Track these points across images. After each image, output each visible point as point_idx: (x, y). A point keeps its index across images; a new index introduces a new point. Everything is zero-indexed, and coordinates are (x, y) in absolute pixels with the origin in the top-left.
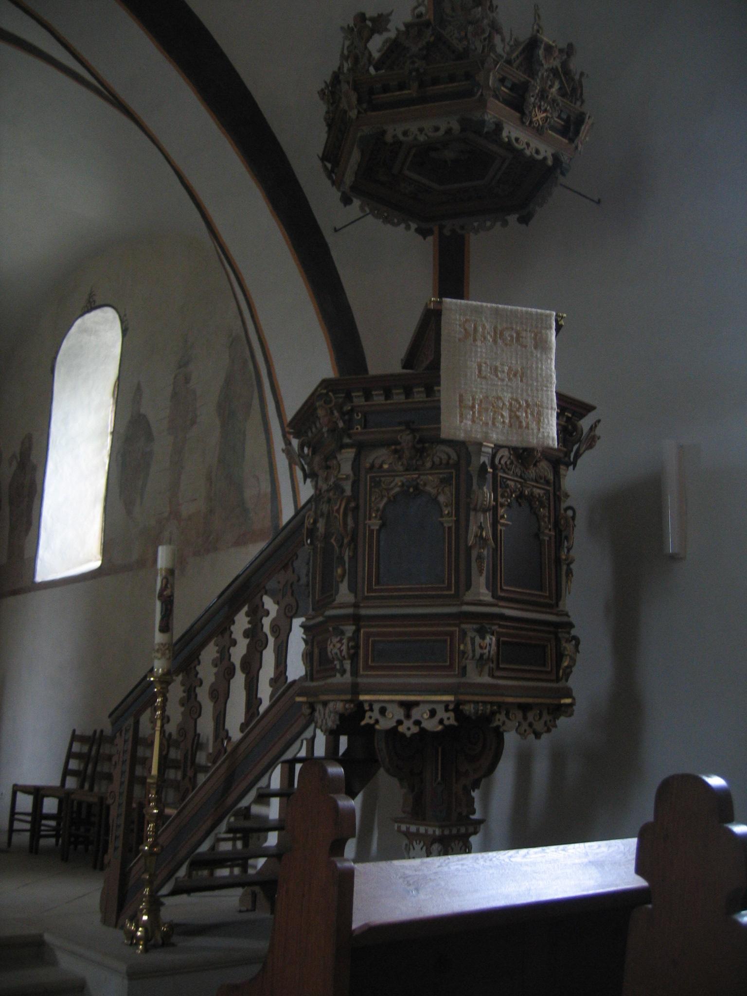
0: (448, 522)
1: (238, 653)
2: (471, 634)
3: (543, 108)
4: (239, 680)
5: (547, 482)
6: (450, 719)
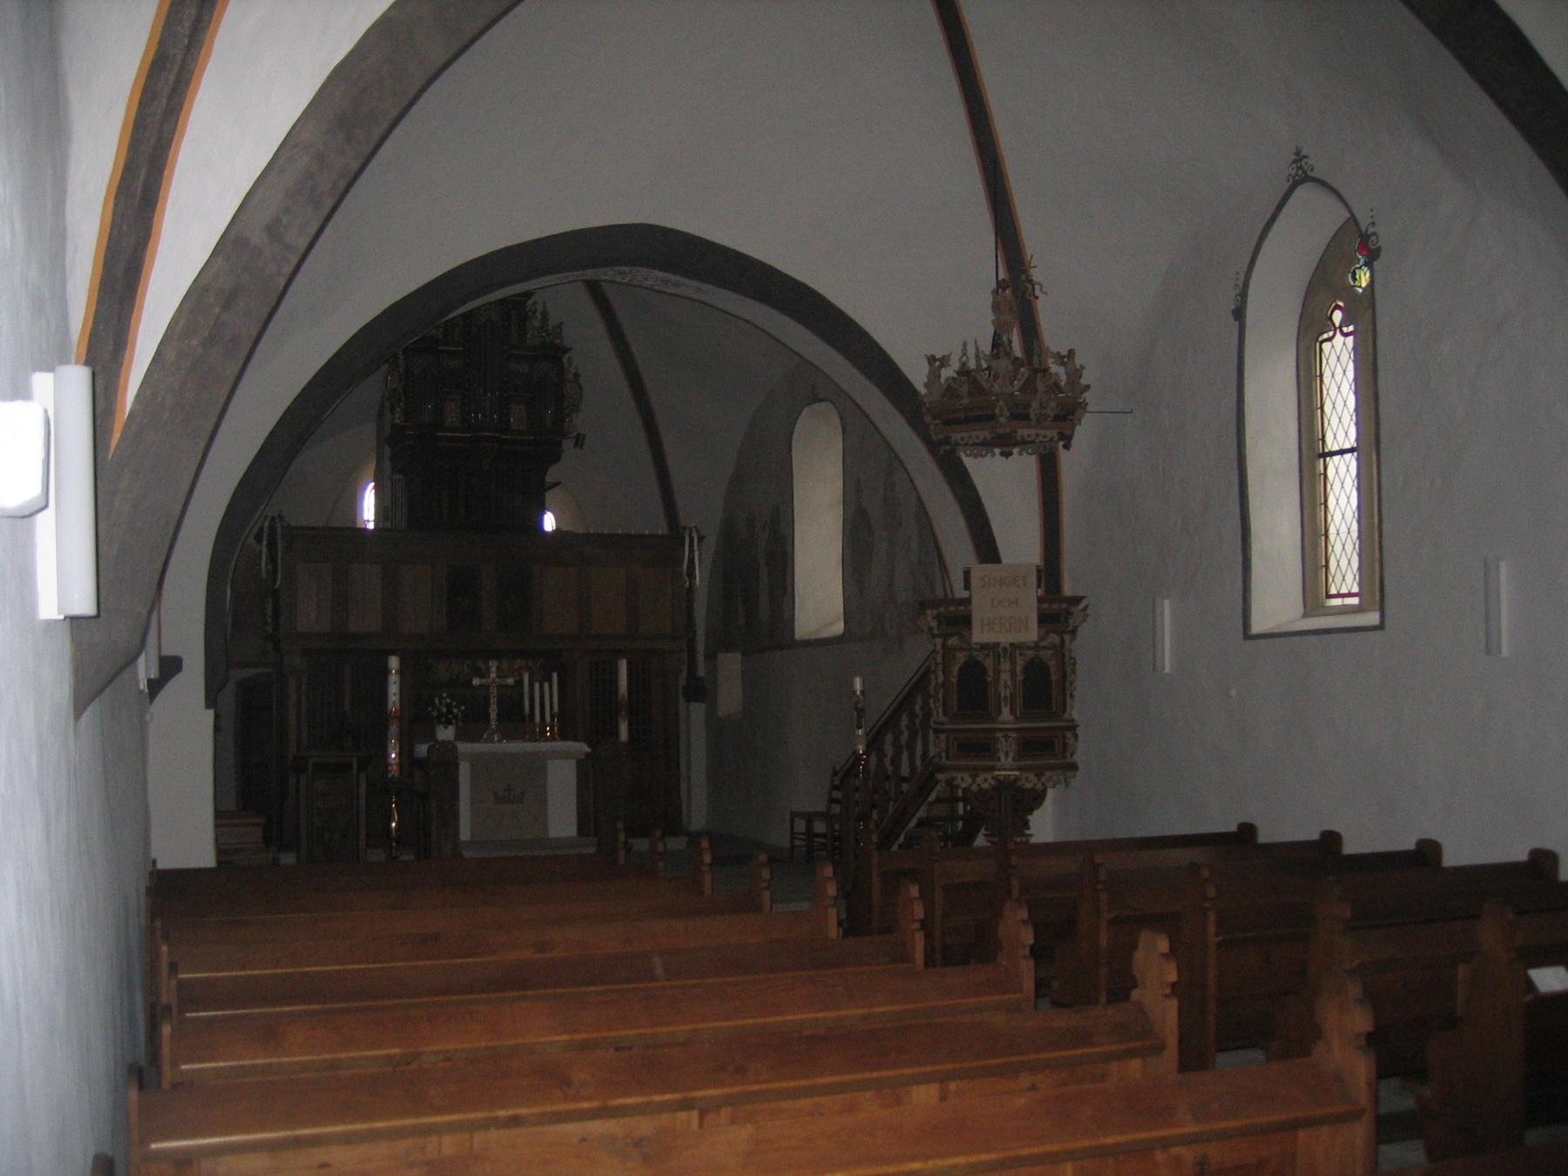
1: (904, 739)
4: (905, 756)
6: (993, 782)
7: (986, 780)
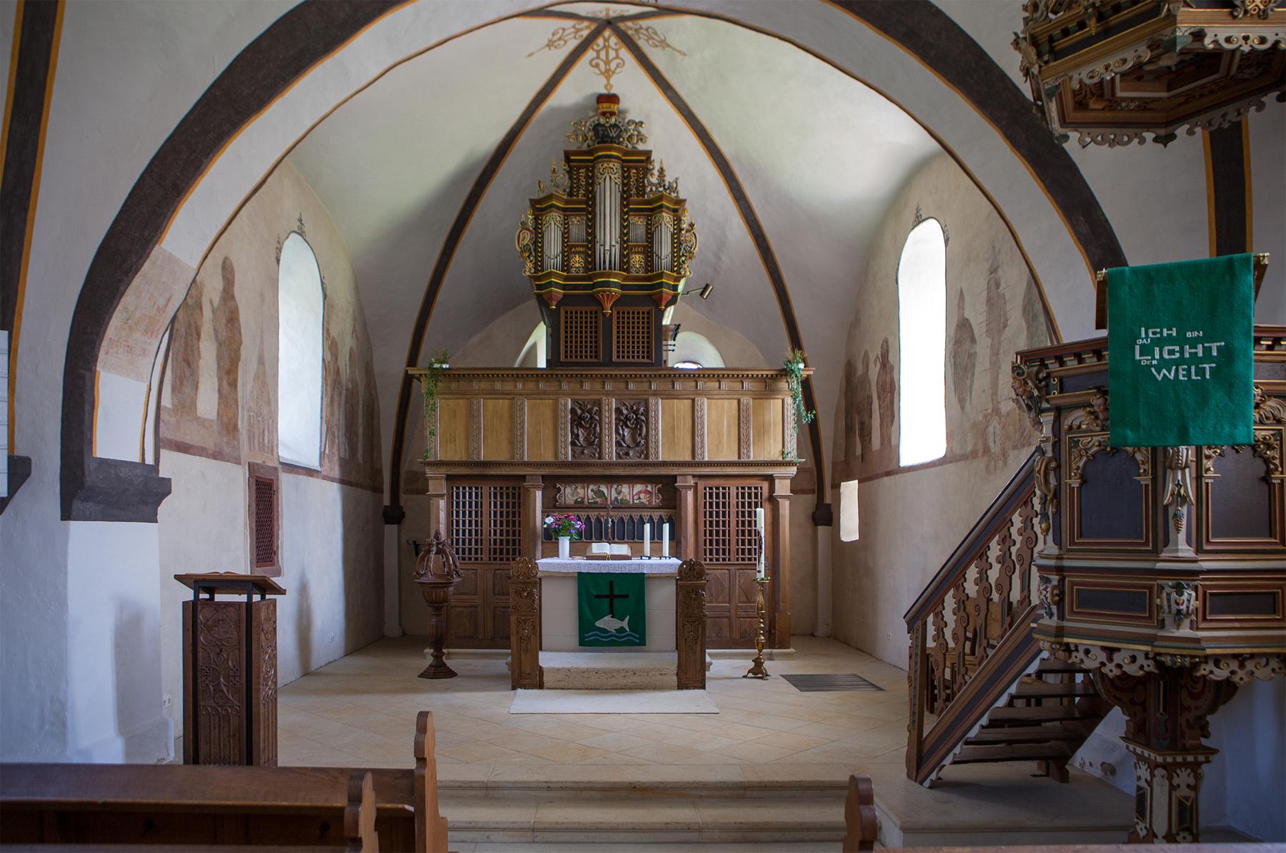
0: (1145, 480)
1: (994, 575)
2: (1167, 590)
6: (1150, 666)
7: (1134, 659)
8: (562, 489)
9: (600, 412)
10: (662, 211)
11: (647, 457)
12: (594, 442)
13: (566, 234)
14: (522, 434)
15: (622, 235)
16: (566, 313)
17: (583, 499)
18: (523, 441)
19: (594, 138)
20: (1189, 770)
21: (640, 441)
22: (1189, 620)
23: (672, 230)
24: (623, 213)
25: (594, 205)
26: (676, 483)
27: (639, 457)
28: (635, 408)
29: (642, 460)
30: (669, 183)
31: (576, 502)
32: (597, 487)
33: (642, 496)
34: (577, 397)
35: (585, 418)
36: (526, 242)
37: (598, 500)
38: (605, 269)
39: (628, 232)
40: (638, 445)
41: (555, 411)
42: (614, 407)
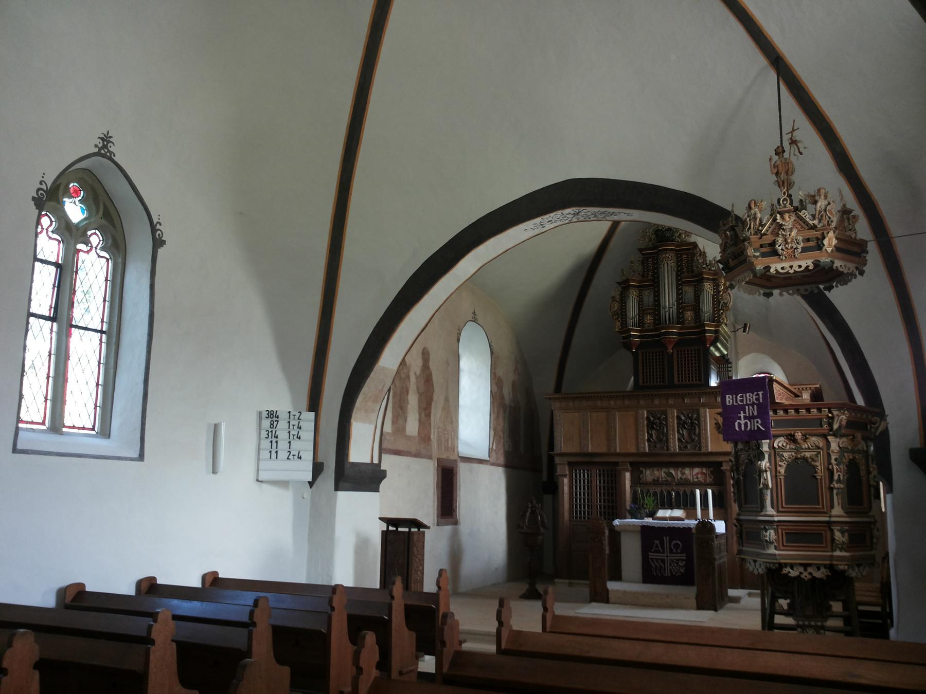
3: (789, 248)
5: (818, 448)
8: (644, 471)
9: (666, 419)
10: (703, 282)
11: (700, 449)
12: (663, 439)
13: (640, 303)
14: (615, 435)
15: (678, 299)
16: (643, 353)
17: (658, 478)
18: (616, 439)
19: (656, 239)
20: (813, 630)
21: (694, 439)
22: (773, 546)
23: (712, 293)
24: (678, 285)
25: (658, 282)
26: (722, 467)
27: (695, 449)
28: (690, 415)
29: (697, 451)
30: (710, 261)
31: (654, 480)
32: (668, 469)
33: (699, 476)
34: (650, 409)
35: (656, 424)
36: (615, 309)
37: (669, 479)
38: (666, 323)
39: (682, 297)
40: (693, 440)
41: (636, 419)
42: (676, 415)
